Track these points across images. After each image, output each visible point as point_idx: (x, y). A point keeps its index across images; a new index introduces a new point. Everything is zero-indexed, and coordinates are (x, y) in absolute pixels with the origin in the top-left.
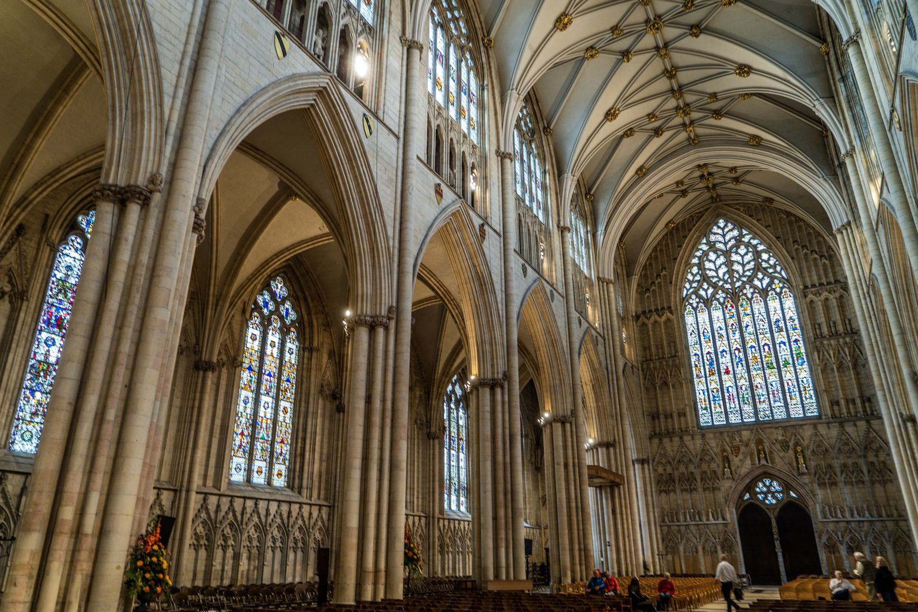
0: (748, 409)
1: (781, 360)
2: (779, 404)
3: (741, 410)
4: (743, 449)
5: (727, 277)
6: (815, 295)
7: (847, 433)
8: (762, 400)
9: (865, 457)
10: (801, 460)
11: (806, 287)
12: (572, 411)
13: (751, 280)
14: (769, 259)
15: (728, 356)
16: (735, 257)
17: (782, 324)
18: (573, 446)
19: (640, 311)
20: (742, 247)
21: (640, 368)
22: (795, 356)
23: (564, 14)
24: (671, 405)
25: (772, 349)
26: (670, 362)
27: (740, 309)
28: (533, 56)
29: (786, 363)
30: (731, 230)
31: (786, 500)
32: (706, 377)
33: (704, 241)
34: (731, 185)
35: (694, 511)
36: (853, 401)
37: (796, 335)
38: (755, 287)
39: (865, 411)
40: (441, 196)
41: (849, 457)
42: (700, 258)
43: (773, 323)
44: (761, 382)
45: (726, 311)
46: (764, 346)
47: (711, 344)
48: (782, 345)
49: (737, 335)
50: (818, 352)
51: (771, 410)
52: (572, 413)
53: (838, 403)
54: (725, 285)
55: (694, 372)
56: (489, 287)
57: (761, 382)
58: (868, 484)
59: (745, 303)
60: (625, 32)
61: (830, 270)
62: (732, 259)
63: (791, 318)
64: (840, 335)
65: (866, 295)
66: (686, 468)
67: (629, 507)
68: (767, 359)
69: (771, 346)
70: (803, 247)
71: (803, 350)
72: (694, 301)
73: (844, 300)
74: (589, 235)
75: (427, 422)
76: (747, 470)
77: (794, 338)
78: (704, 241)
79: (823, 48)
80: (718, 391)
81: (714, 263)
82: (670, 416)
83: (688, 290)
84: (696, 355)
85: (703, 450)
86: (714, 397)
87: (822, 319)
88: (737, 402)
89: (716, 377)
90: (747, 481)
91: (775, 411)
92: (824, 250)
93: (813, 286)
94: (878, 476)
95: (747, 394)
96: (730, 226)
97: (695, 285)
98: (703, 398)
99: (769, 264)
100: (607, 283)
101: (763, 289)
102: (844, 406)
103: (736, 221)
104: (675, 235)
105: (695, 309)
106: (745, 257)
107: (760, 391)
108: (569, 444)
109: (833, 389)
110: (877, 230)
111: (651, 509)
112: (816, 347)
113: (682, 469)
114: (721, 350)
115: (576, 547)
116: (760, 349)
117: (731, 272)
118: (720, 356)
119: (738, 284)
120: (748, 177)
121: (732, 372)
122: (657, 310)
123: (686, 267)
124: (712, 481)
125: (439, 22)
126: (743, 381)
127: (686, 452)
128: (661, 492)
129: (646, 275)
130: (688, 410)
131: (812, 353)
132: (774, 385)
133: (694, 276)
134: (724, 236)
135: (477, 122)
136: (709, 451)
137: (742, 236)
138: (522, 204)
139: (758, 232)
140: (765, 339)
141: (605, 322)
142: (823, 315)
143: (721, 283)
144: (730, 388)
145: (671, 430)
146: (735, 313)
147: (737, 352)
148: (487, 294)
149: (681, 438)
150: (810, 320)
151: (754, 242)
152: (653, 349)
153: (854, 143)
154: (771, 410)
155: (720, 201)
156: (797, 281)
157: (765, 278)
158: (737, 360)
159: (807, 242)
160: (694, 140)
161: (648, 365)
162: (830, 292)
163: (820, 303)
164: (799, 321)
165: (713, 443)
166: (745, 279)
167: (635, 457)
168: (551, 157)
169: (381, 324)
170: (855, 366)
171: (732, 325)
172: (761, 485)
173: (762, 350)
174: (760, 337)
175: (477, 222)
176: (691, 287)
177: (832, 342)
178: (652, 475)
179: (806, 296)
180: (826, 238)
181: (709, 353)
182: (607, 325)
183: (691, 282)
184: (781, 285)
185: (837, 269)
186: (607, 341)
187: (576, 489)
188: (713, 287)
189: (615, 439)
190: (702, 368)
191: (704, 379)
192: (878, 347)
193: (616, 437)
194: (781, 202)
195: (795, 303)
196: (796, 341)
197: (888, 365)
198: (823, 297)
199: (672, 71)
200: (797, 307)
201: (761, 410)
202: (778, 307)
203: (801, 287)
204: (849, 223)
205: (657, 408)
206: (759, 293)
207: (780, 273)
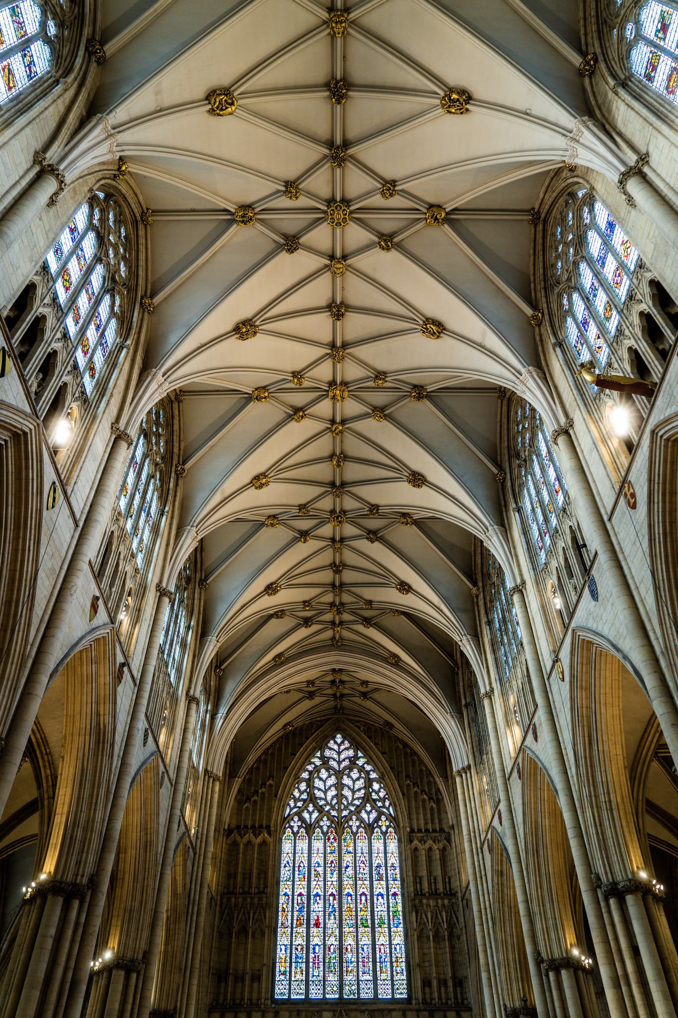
0: (332, 978)
1: (376, 918)
5: (335, 801)
6: (420, 841)
8: (350, 969)
11: (412, 831)
13: (359, 809)
15: (321, 902)
19: (233, 826)
20: (355, 771)
21: (218, 902)
22: (391, 914)
23: (264, 475)
24: (245, 962)
25: (368, 901)
26: (256, 900)
27: (343, 844)
28: (222, 501)
30: (347, 749)
32: (292, 928)
33: (318, 754)
34: (357, 700)
36: (445, 983)
37: (396, 887)
38: (362, 820)
39: (456, 998)
42: (310, 773)
45: (328, 844)
46: (361, 895)
48: (380, 897)
49: (335, 876)
51: (358, 985)
54: (331, 811)
55: (280, 918)
60: (311, 513)
61: (436, 815)
62: (344, 782)
64: (439, 894)
65: (479, 850)
68: (362, 913)
70: (414, 784)
71: (400, 909)
72: (296, 824)
73: (447, 853)
74: (208, 715)
77: (393, 891)
78: (318, 754)
79: (474, 590)
80: (302, 949)
81: (325, 782)
82: (239, 978)
83: (291, 809)
87: (424, 873)
88: (322, 969)
89: (302, 930)
91: (362, 986)
92: (433, 792)
93: (420, 831)
95: (334, 956)
97: (300, 804)
98: (283, 957)
100: (214, 780)
101: (369, 825)
102: (436, 988)
104: (291, 740)
105: (295, 834)
106: (356, 783)
107: (350, 956)
109: (427, 964)
110: (509, 779)
114: (314, 893)
116: (356, 899)
117: (339, 796)
118: (312, 901)
119: (345, 813)
120: (376, 696)
121: (322, 926)
122: (253, 827)
123: (294, 780)
129: (250, 780)
130: (264, 972)
131: (412, 912)
132: (365, 950)
134: (339, 753)
135: (146, 545)
137: (356, 757)
139: (374, 757)
142: (425, 867)
143: (327, 808)
144: (317, 947)
147: (331, 898)
148: (102, 756)
151: (368, 768)
152: (239, 878)
153: (494, 685)
154: (358, 985)
155: (343, 713)
156: (404, 822)
157: (373, 811)
158: (330, 910)
159: (419, 780)
160: (338, 642)
161: (229, 899)
162: (434, 841)
163: (423, 852)
166: (353, 809)
168: (199, 614)
170: (451, 936)
171: (332, 862)
173: (359, 901)
174: (359, 882)
175: (120, 659)
176: (295, 807)
177: (431, 902)
179: (411, 841)
180: (437, 779)
181: (300, 895)
182: (202, 835)
183: (296, 800)
184: (388, 823)
185: (443, 816)
188: (319, 811)
190: (290, 914)
191: (289, 930)
192: (487, 915)
195: (399, 847)
196: (395, 894)
197: (496, 940)
198: (427, 846)
199: (340, 566)
200: (400, 853)
201: (347, 983)
202: (382, 848)
203: (408, 829)
204: (469, 767)
205: (228, 964)
206: (365, 828)
207: (388, 809)
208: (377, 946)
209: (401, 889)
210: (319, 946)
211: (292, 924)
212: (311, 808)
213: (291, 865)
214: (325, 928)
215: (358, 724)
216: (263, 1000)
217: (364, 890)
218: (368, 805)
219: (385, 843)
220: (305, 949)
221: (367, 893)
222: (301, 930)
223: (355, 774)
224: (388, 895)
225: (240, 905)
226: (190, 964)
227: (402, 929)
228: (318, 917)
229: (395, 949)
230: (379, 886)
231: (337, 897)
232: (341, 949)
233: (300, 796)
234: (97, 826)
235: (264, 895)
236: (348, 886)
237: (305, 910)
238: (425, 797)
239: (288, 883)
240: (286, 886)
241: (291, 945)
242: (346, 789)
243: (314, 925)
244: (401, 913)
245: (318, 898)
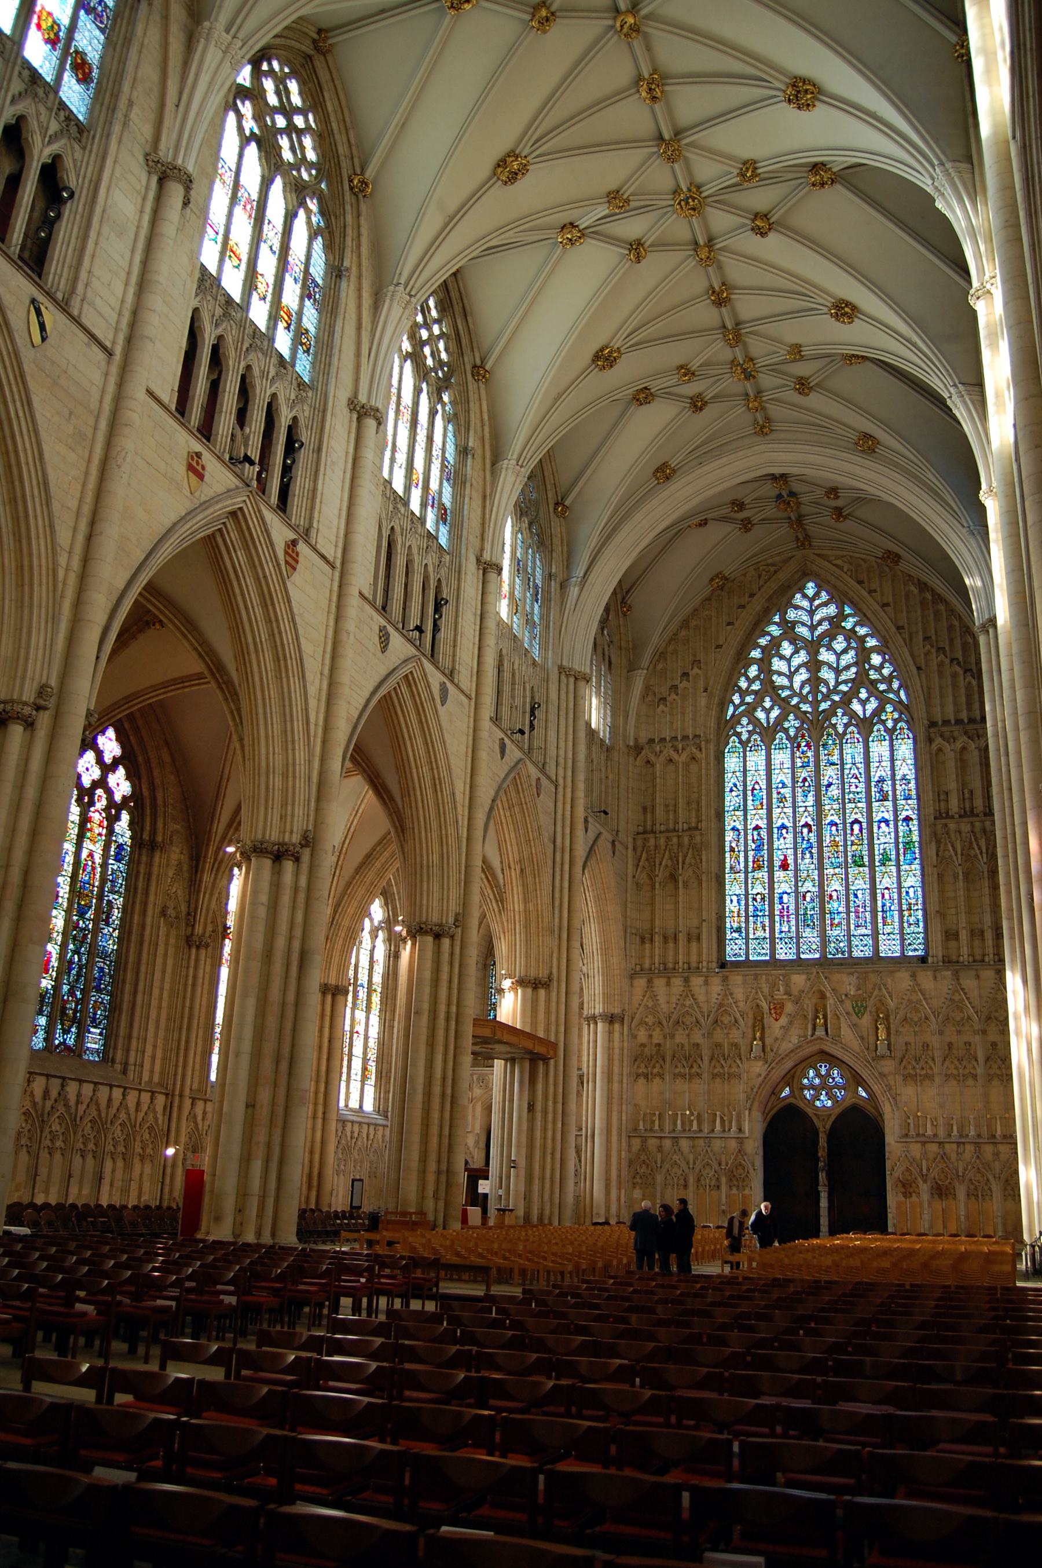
0: (810, 935)
1: (877, 853)
2: (863, 931)
3: (798, 937)
4: (789, 1008)
7: (963, 989)
8: (836, 921)
9: (984, 1032)
10: (882, 1035)
11: (933, 724)
12: (457, 915)
13: (847, 699)
14: (882, 666)
15: (790, 837)
16: (825, 656)
17: (887, 787)
18: (450, 982)
20: (840, 638)
21: (630, 846)
22: (901, 846)
23: (512, 154)
24: (677, 917)
26: (686, 840)
27: (822, 752)
28: (447, 224)
29: (885, 860)
30: (825, 604)
31: (849, 1102)
32: (746, 873)
33: (777, 619)
35: (692, 1114)
36: (982, 932)
37: (909, 809)
38: (853, 714)
40: (201, 477)
41: (959, 1032)
42: (764, 649)
43: (873, 784)
44: (839, 888)
45: (798, 754)
46: (853, 823)
47: (763, 812)
48: (883, 825)
49: (811, 800)
50: (938, 842)
51: (849, 941)
52: (456, 920)
53: (956, 936)
54: (801, 705)
55: (728, 860)
56: (292, 664)
57: (839, 888)
58: (981, 1081)
59: (830, 742)
60: (633, 204)
62: (820, 658)
63: (904, 777)
64: (977, 815)
66: (688, 1035)
67: (560, 1100)
68: (854, 848)
69: (864, 825)
71: (915, 838)
72: (744, 730)
75: (189, 914)
76: (791, 1046)
77: (904, 814)
78: (777, 619)
80: (763, 899)
81: (789, 661)
83: (736, 707)
84: (734, 829)
85: (721, 1005)
86: (756, 909)
87: (952, 785)
88: (793, 922)
90: (789, 1064)
91: (855, 942)
94: (999, 1068)
95: (811, 907)
96: (824, 596)
97: (749, 699)
98: (736, 910)
99: (881, 674)
103: (835, 587)
106: (842, 657)
107: (835, 905)
108: (444, 976)
111: (615, 1107)
112: (935, 834)
113: (680, 1037)
114: (779, 824)
115: (432, 1166)
117: (815, 681)
118: (775, 836)
119: (824, 706)
121: (792, 867)
124: (729, 1062)
125: (252, 133)
126: (808, 886)
127: (691, 1006)
128: (638, 1076)
130: (704, 930)
131: (930, 842)
132: (860, 896)
133: (751, 681)
134: (811, 613)
136: (731, 1007)
137: (841, 616)
138: (402, 510)
139: (869, 614)
140: (856, 812)
141: (562, 752)
143: (795, 701)
144: (785, 897)
145: (671, 965)
146: (812, 759)
147: (805, 830)
149: (687, 980)
150: (933, 785)
151: (862, 631)
152: (659, 811)
156: (920, 712)
159: (947, 642)
164: (917, 783)
165: (739, 994)
166: (837, 698)
167: (599, 1009)
169: (19, 718)
171: (805, 780)
172: (811, 1073)
173: (849, 832)
174: (849, 806)
176: (742, 703)
178: (625, 1044)
179: (930, 741)
182: (565, 759)
184: (896, 715)
186: (560, 789)
187: (445, 1061)
188: (780, 708)
189: (551, 974)
190: (742, 854)
193: (555, 971)
194: (911, 565)
195: (915, 750)
196: (907, 819)
198: (958, 745)
199: (722, 291)
200: (916, 758)
202: (886, 754)
203: (926, 722)
205: (652, 921)
206: (856, 726)
208: (878, 891)
209: (918, 810)
210: (789, 894)
211: (746, 866)
212: (767, 704)
213: (741, 788)
214: (796, 870)
215: (839, 562)
216: (705, 964)
217: (856, 816)
218: (863, 690)
219: (891, 746)
220: (767, 899)
221: (861, 820)
222: (760, 875)
224: (896, 821)
225: (663, 847)
226: (566, 925)
227: (918, 867)
228: (785, 856)
229: (907, 893)
230: (882, 809)
231: (814, 828)
232: (822, 896)
233: (749, 686)
234: (301, 769)
235: (698, 832)
236: (832, 812)
237: (766, 847)
238: (957, 669)
239: (737, 813)
240: (735, 818)
241: (747, 895)
242: (825, 668)
243: (780, 867)
244: (917, 844)
245: (784, 831)
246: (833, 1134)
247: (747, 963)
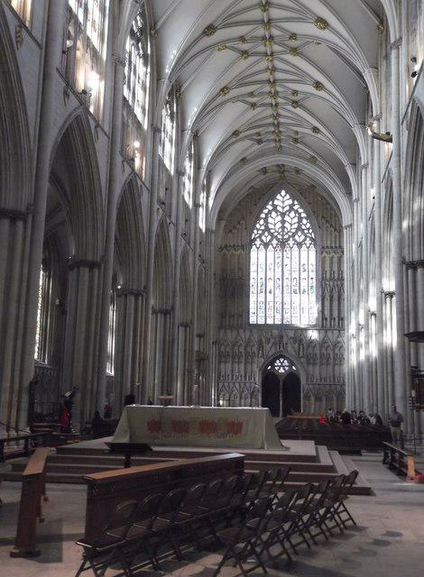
0: (278, 316)
4: (272, 341)
9: (334, 350)
16: (287, 218)
29: (304, 291)
37: (313, 275)
78: (270, 203)
87: (327, 269)
89: (263, 294)
95: (279, 306)
97: (260, 232)
117: (283, 227)
119: (286, 237)
134: (283, 202)
137: (293, 205)
151: (300, 211)
183: (258, 230)
212: (266, 234)
223: (292, 214)
246: (285, 382)
247: (257, 326)
